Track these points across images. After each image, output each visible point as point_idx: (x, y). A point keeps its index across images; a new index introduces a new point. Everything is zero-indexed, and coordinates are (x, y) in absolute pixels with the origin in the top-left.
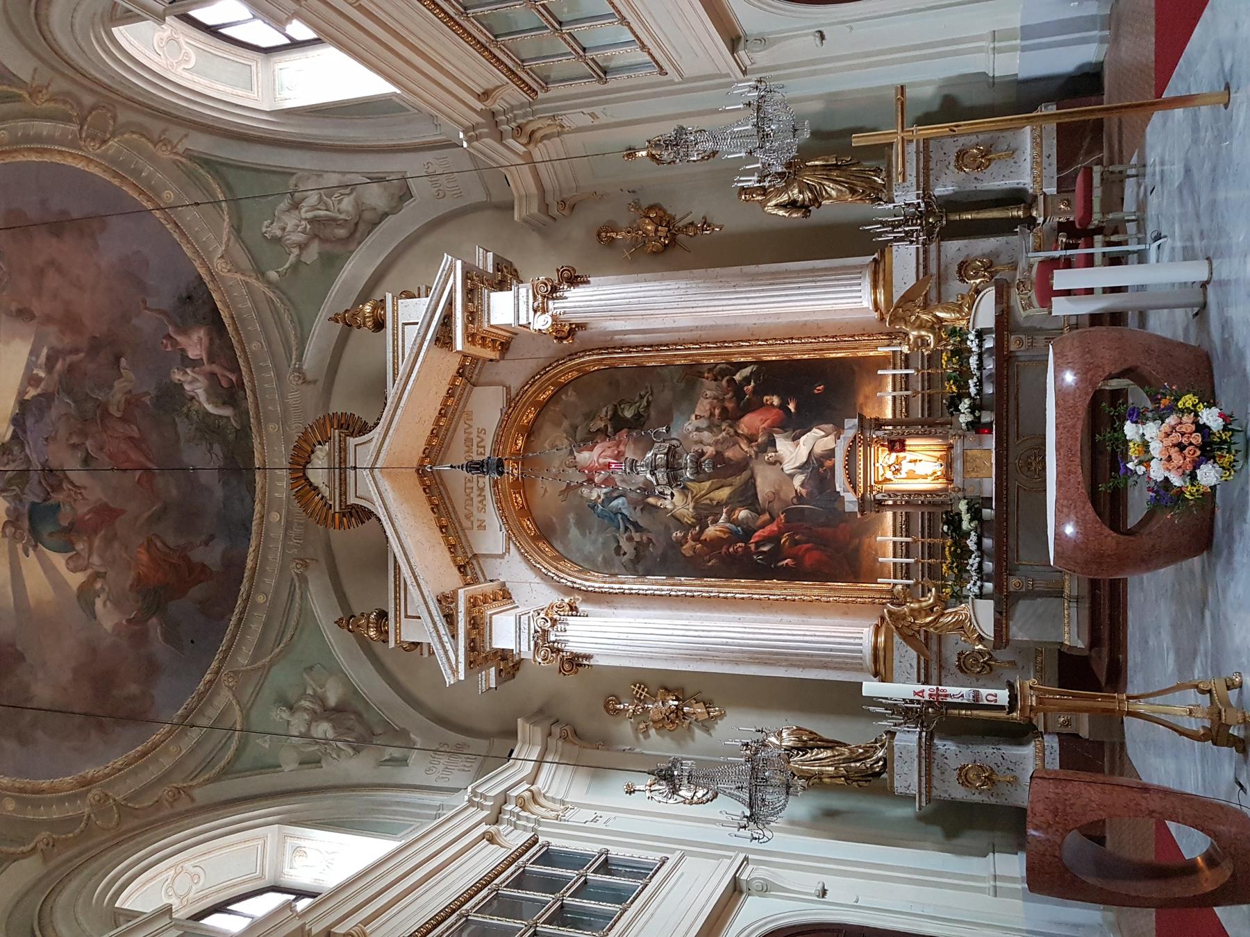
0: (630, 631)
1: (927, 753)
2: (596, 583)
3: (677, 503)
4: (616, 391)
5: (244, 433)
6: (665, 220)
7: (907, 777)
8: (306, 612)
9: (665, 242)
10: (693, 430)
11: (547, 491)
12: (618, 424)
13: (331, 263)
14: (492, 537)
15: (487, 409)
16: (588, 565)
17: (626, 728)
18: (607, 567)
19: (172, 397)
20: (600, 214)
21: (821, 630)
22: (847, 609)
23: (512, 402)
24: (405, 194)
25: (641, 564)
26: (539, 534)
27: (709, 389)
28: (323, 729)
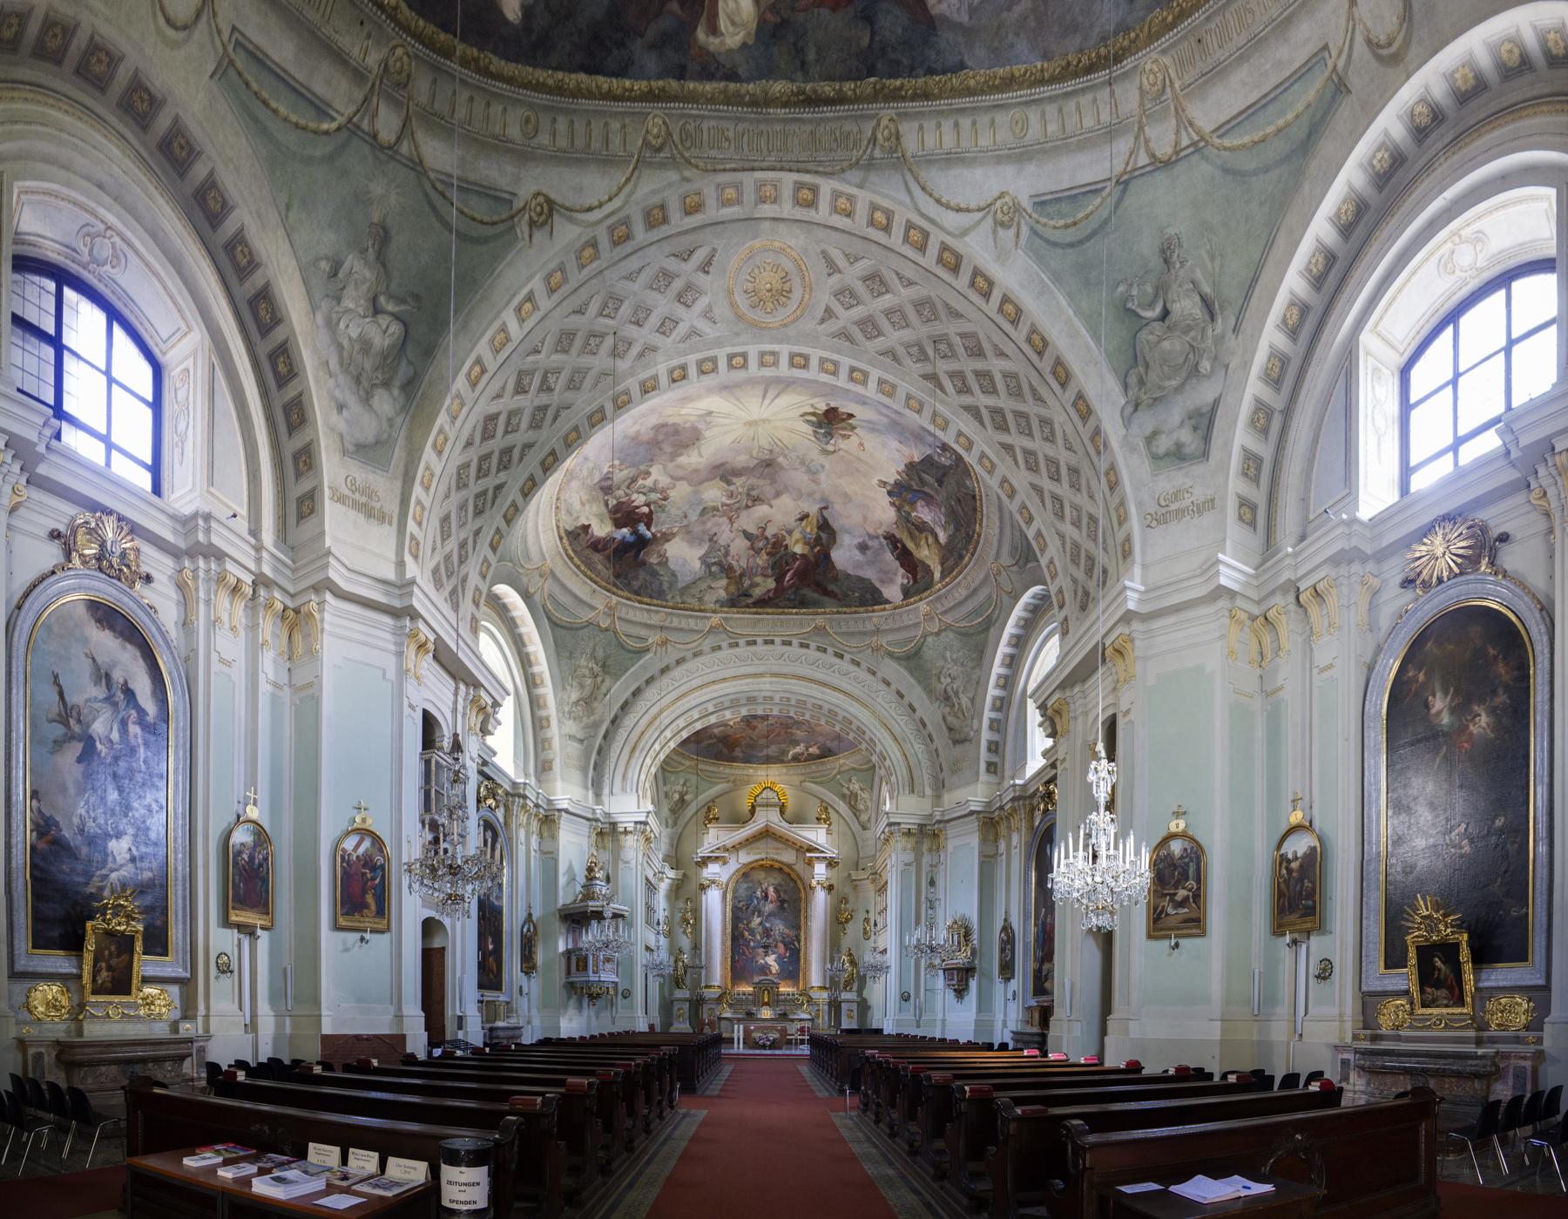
0: (714, 905)
1: (685, 1000)
2: (729, 896)
3: (757, 920)
4: (792, 898)
5: (782, 762)
6: (847, 921)
7: (679, 994)
8: (716, 784)
9: (838, 920)
10: (779, 927)
11: (761, 875)
12: (782, 902)
13: (843, 797)
14: (745, 858)
15: (788, 857)
16: (735, 891)
17: (682, 905)
18: (734, 898)
19: (796, 743)
20: (852, 899)
21: (718, 972)
22: (724, 977)
23: (790, 866)
24: (864, 828)
25: (736, 911)
26: (746, 874)
27: (792, 933)
28: (677, 796)
